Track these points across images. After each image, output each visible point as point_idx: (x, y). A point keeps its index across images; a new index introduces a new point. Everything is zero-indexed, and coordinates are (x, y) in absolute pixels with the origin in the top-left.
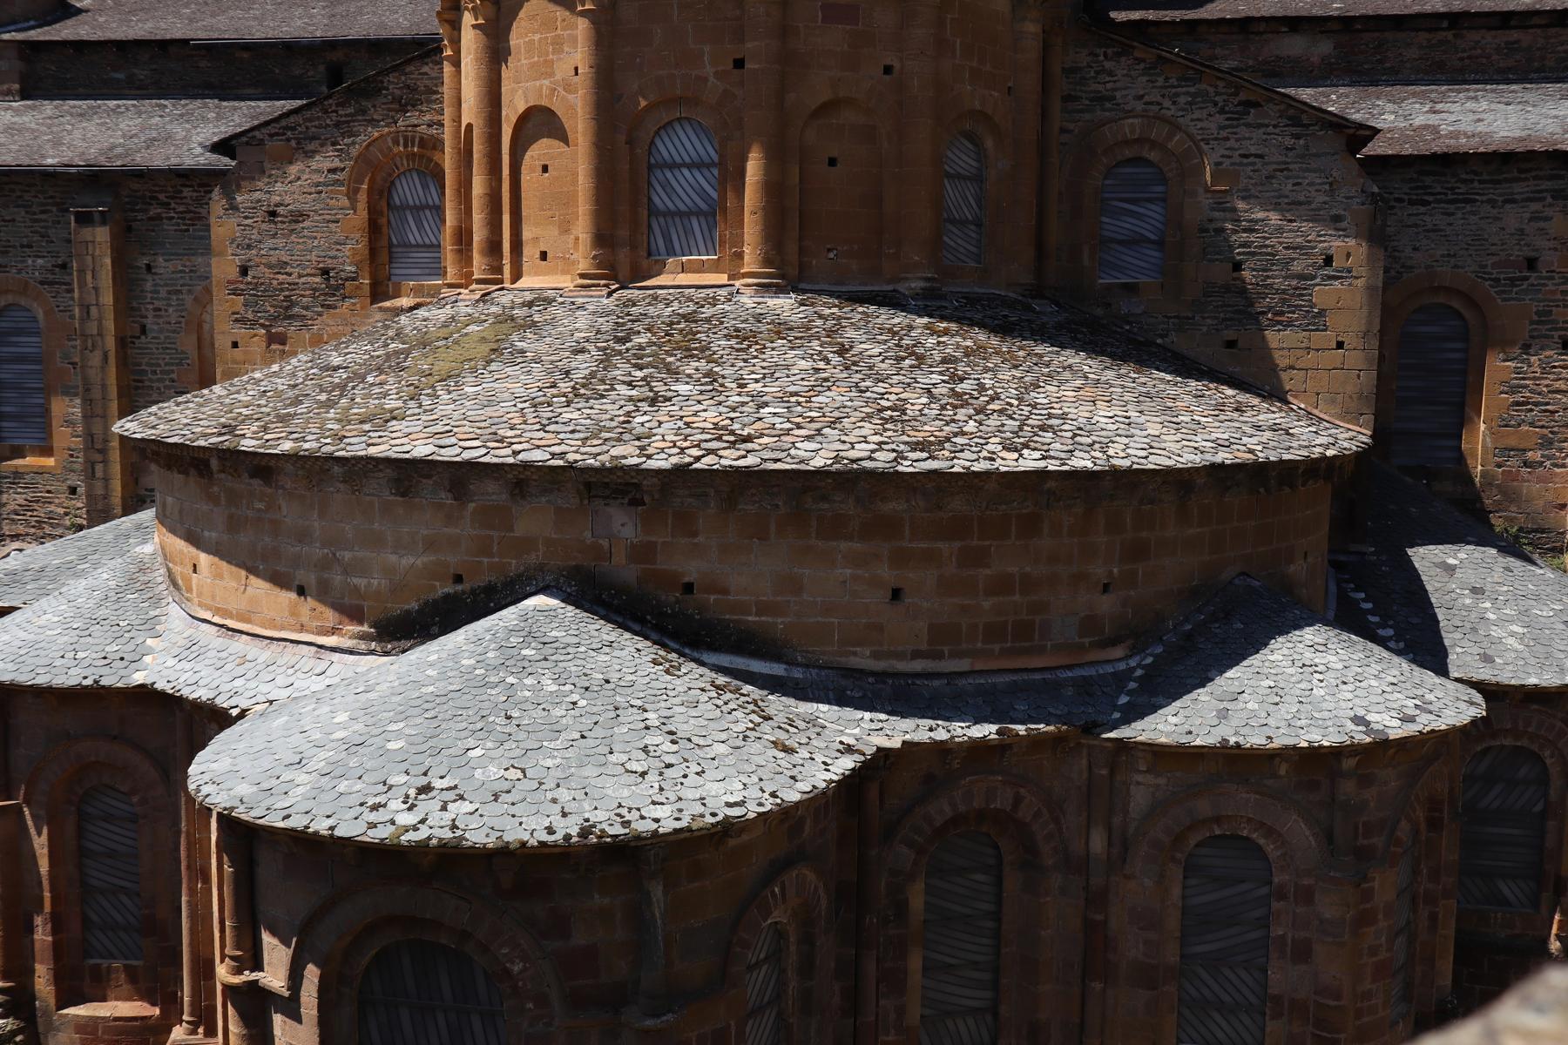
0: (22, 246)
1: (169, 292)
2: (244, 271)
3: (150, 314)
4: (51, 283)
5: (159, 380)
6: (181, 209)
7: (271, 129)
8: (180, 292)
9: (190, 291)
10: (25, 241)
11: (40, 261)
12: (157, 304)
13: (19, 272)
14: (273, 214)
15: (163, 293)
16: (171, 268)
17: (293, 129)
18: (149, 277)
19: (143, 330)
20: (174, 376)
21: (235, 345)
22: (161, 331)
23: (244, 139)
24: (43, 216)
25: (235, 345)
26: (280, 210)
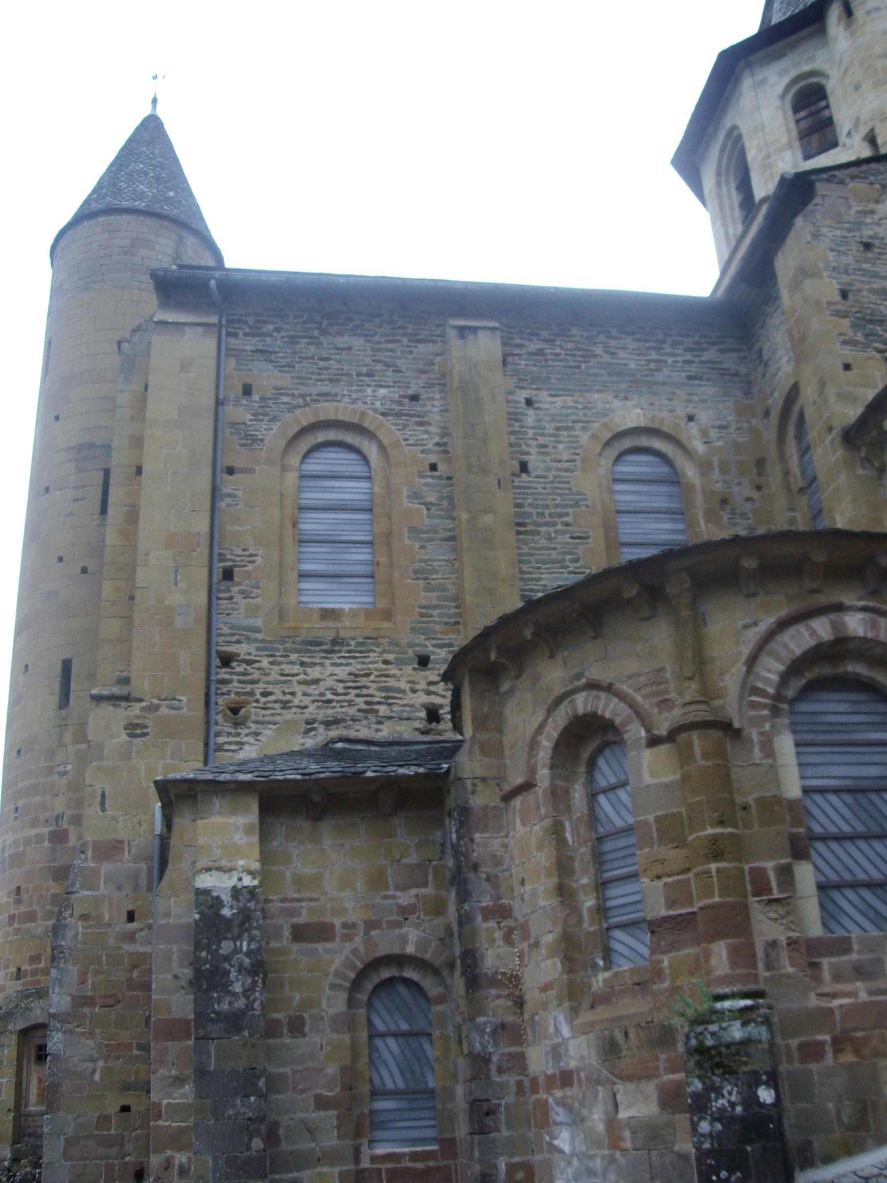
0: (359, 374)
1: (558, 429)
2: (844, 294)
3: (534, 450)
4: (398, 415)
5: (546, 524)
6: (570, 345)
7: (853, 171)
8: (572, 428)
9: (584, 428)
10: (364, 370)
11: (382, 392)
12: (542, 440)
13: (355, 401)
14: (867, 246)
15: (550, 428)
16: (559, 404)
17: (875, 175)
18: (531, 412)
19: (524, 467)
20: (568, 519)
21: (847, 367)
22: (548, 470)
23: (825, 176)
24: (390, 346)
25: (847, 367)
26: (876, 242)
